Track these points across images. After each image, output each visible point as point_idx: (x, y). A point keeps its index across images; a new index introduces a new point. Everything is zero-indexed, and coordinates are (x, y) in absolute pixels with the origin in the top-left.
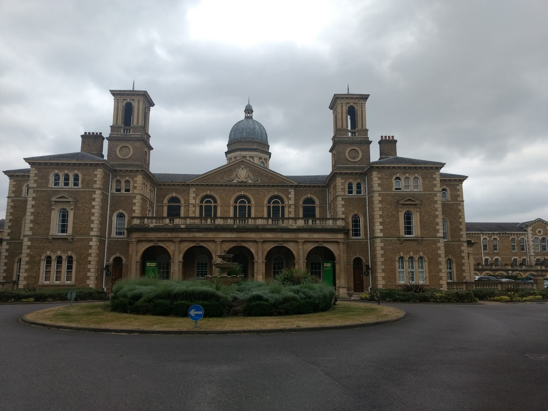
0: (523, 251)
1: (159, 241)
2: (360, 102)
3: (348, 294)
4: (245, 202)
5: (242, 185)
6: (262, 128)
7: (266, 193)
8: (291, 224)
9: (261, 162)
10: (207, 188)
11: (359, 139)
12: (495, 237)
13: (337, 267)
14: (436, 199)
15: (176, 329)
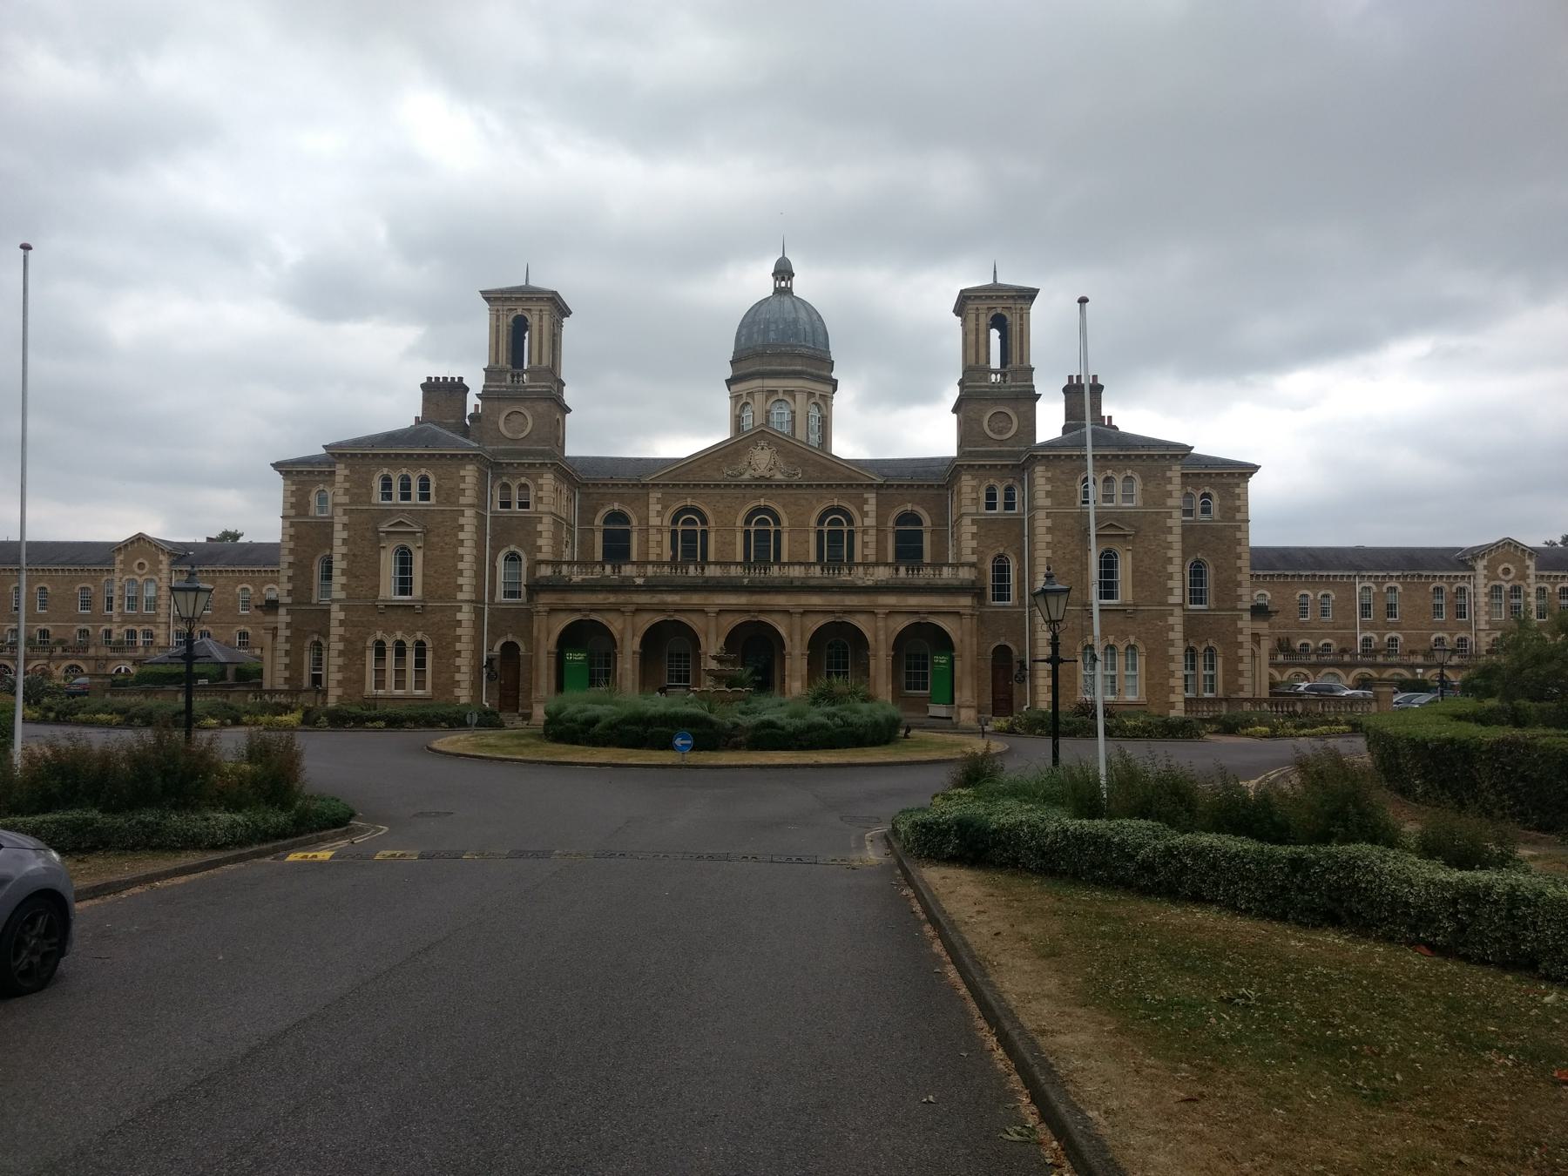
0: (1461, 617)
1: (592, 610)
2: (1019, 306)
3: (979, 721)
4: (766, 522)
5: (763, 484)
6: (815, 317)
7: (814, 502)
8: (860, 576)
9: (814, 403)
10: (686, 491)
11: (1012, 389)
12: (1392, 584)
13: (958, 664)
14: (1170, 522)
15: (659, 763)
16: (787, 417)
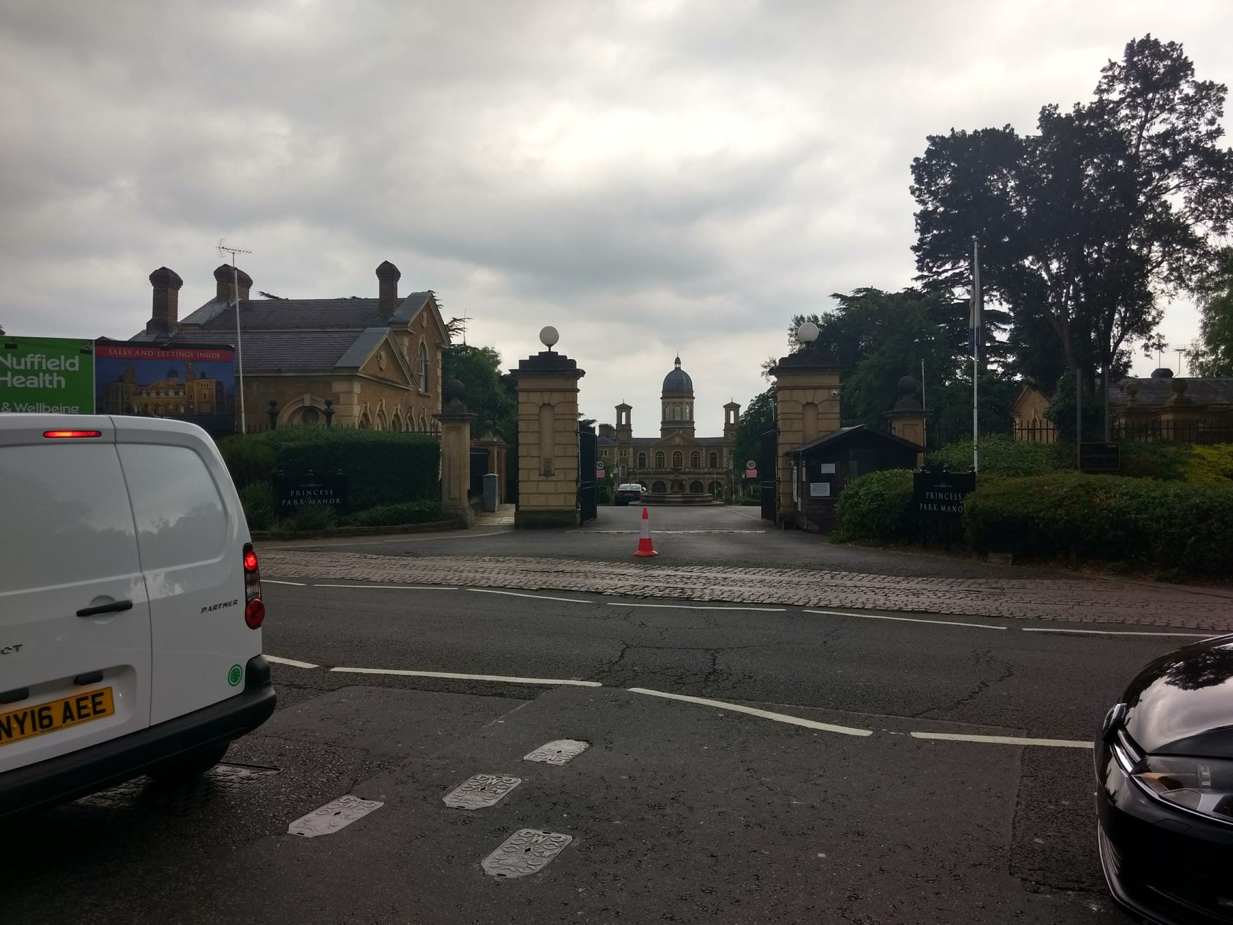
5: (678, 446)
8: (702, 471)
16: (680, 410)
